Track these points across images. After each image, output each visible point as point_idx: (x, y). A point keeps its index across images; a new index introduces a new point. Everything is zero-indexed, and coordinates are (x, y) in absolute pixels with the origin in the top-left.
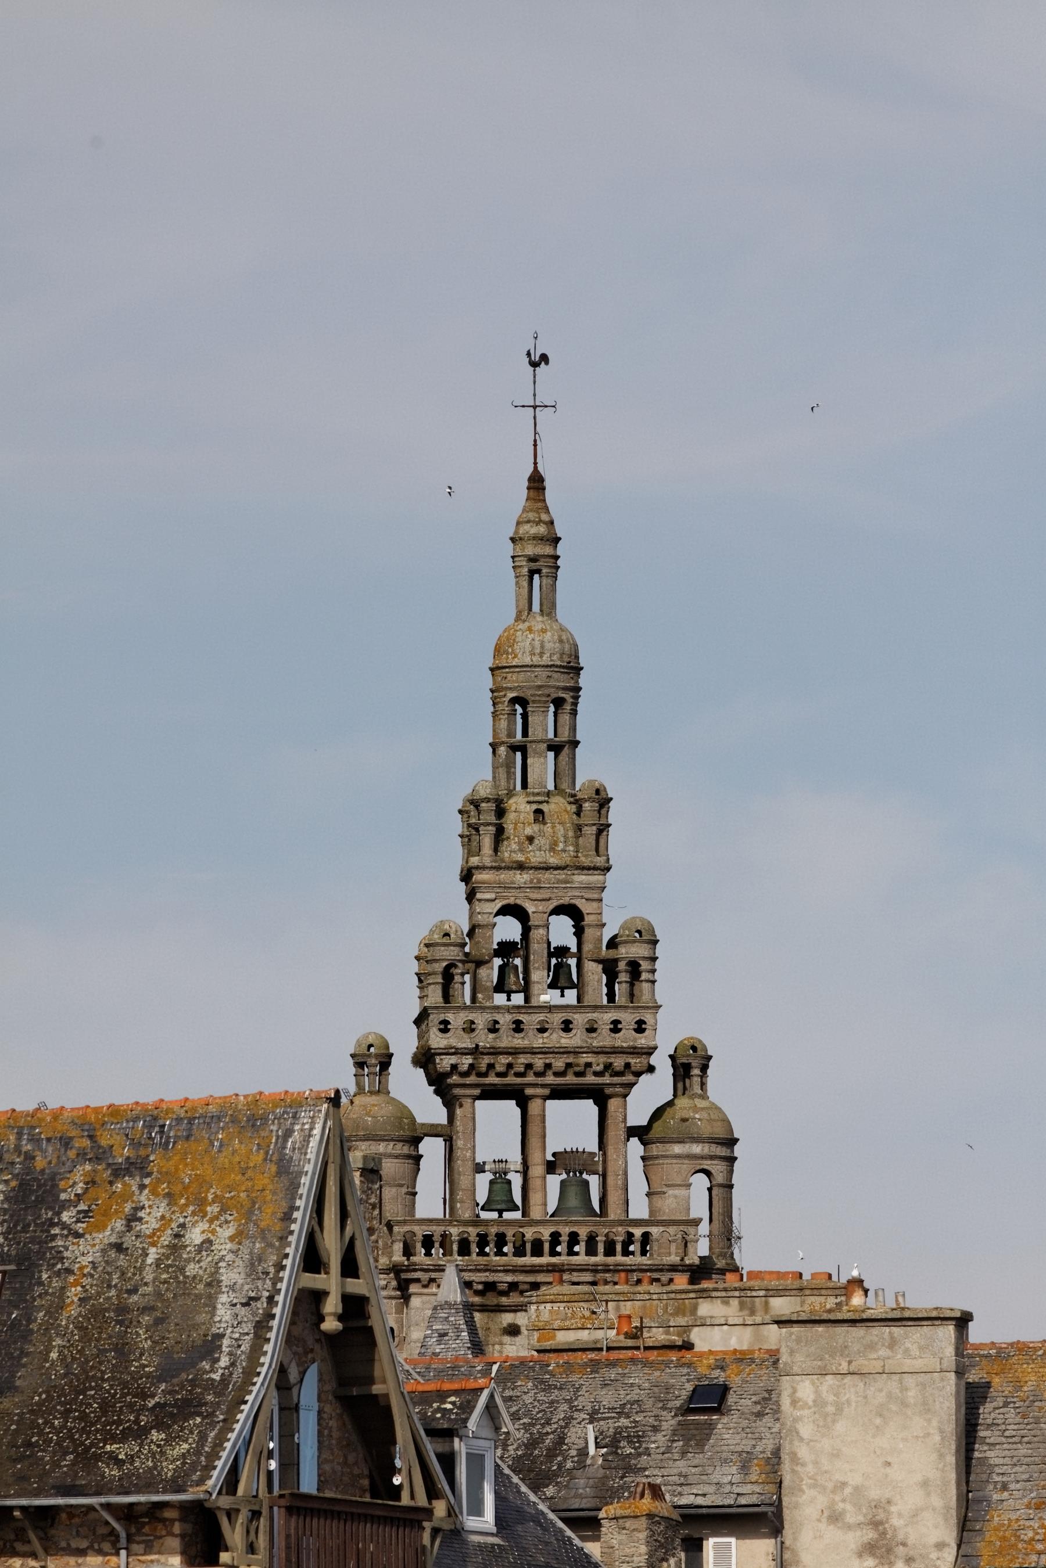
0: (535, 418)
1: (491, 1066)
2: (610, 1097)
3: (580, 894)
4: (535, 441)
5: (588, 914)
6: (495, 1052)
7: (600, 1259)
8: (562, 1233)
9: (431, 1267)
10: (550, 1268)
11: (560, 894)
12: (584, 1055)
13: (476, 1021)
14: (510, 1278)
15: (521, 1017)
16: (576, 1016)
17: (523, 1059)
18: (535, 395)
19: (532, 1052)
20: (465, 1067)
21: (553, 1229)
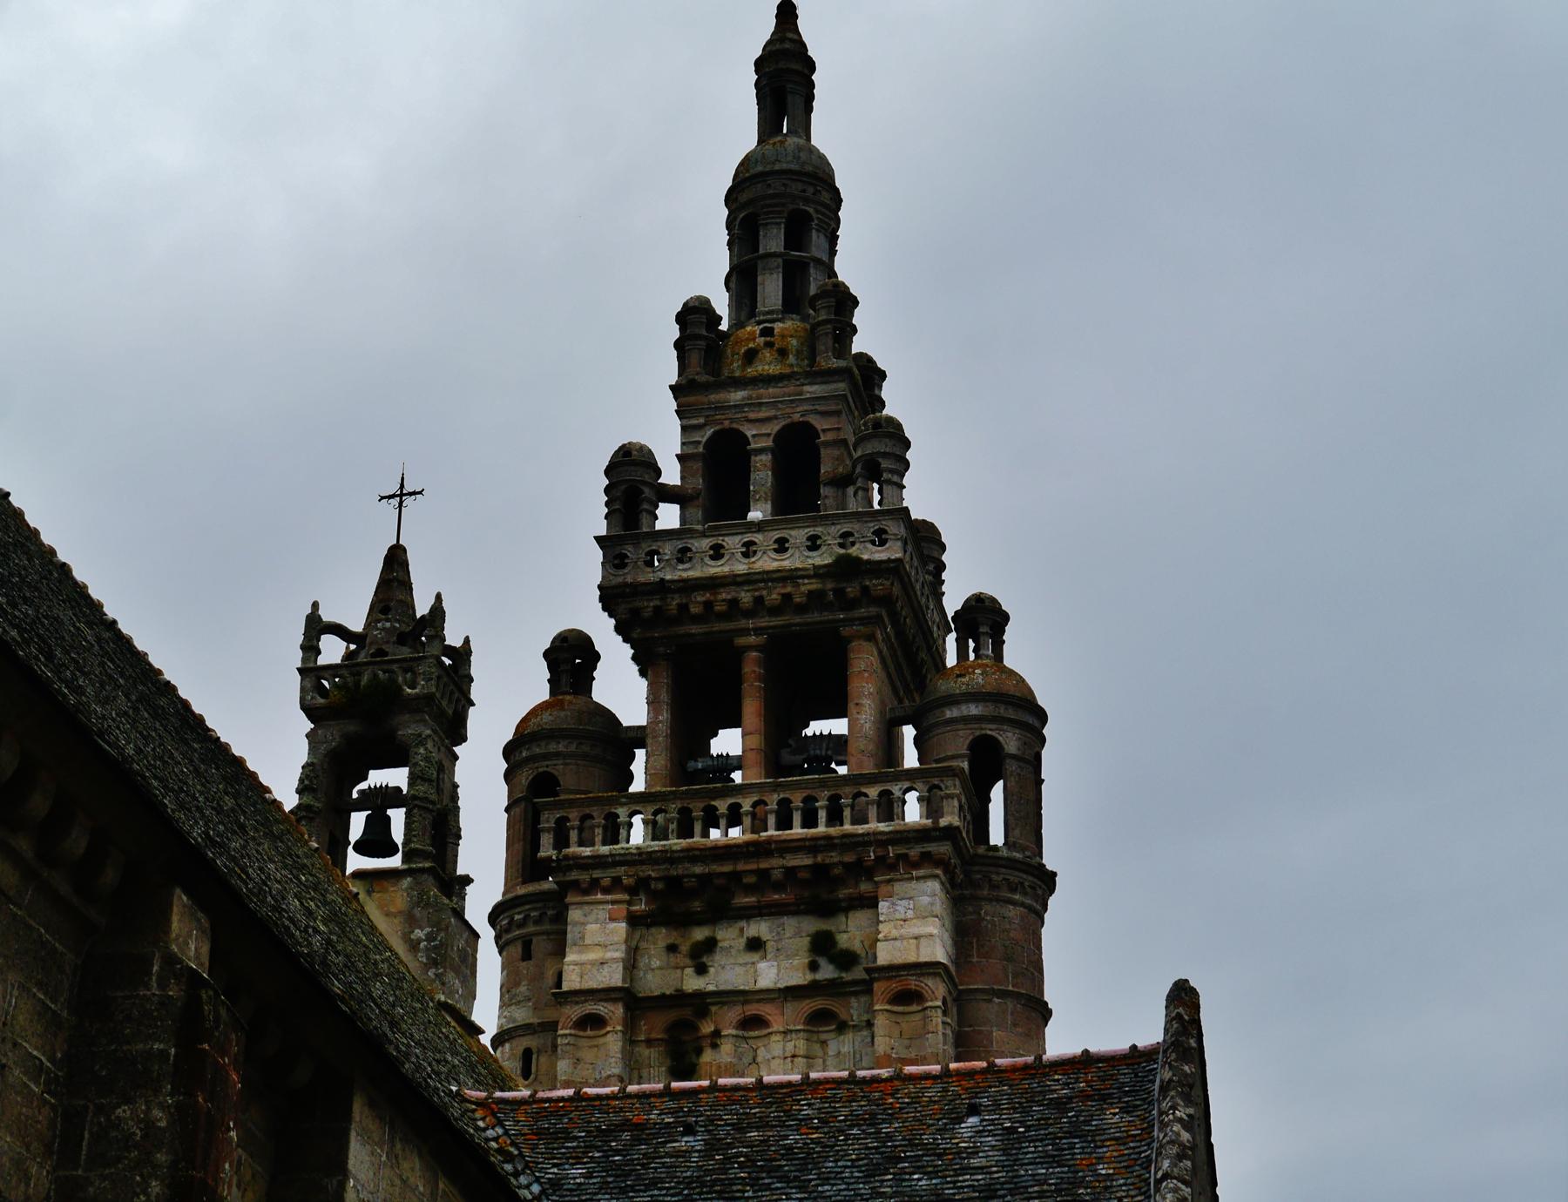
1: (683, 608)
2: (849, 640)
3: (812, 408)
7: (821, 829)
10: (751, 849)
11: (788, 410)
12: (806, 581)
13: (661, 550)
14: (698, 869)
16: (793, 533)
17: (724, 595)
19: (734, 581)
20: (647, 614)
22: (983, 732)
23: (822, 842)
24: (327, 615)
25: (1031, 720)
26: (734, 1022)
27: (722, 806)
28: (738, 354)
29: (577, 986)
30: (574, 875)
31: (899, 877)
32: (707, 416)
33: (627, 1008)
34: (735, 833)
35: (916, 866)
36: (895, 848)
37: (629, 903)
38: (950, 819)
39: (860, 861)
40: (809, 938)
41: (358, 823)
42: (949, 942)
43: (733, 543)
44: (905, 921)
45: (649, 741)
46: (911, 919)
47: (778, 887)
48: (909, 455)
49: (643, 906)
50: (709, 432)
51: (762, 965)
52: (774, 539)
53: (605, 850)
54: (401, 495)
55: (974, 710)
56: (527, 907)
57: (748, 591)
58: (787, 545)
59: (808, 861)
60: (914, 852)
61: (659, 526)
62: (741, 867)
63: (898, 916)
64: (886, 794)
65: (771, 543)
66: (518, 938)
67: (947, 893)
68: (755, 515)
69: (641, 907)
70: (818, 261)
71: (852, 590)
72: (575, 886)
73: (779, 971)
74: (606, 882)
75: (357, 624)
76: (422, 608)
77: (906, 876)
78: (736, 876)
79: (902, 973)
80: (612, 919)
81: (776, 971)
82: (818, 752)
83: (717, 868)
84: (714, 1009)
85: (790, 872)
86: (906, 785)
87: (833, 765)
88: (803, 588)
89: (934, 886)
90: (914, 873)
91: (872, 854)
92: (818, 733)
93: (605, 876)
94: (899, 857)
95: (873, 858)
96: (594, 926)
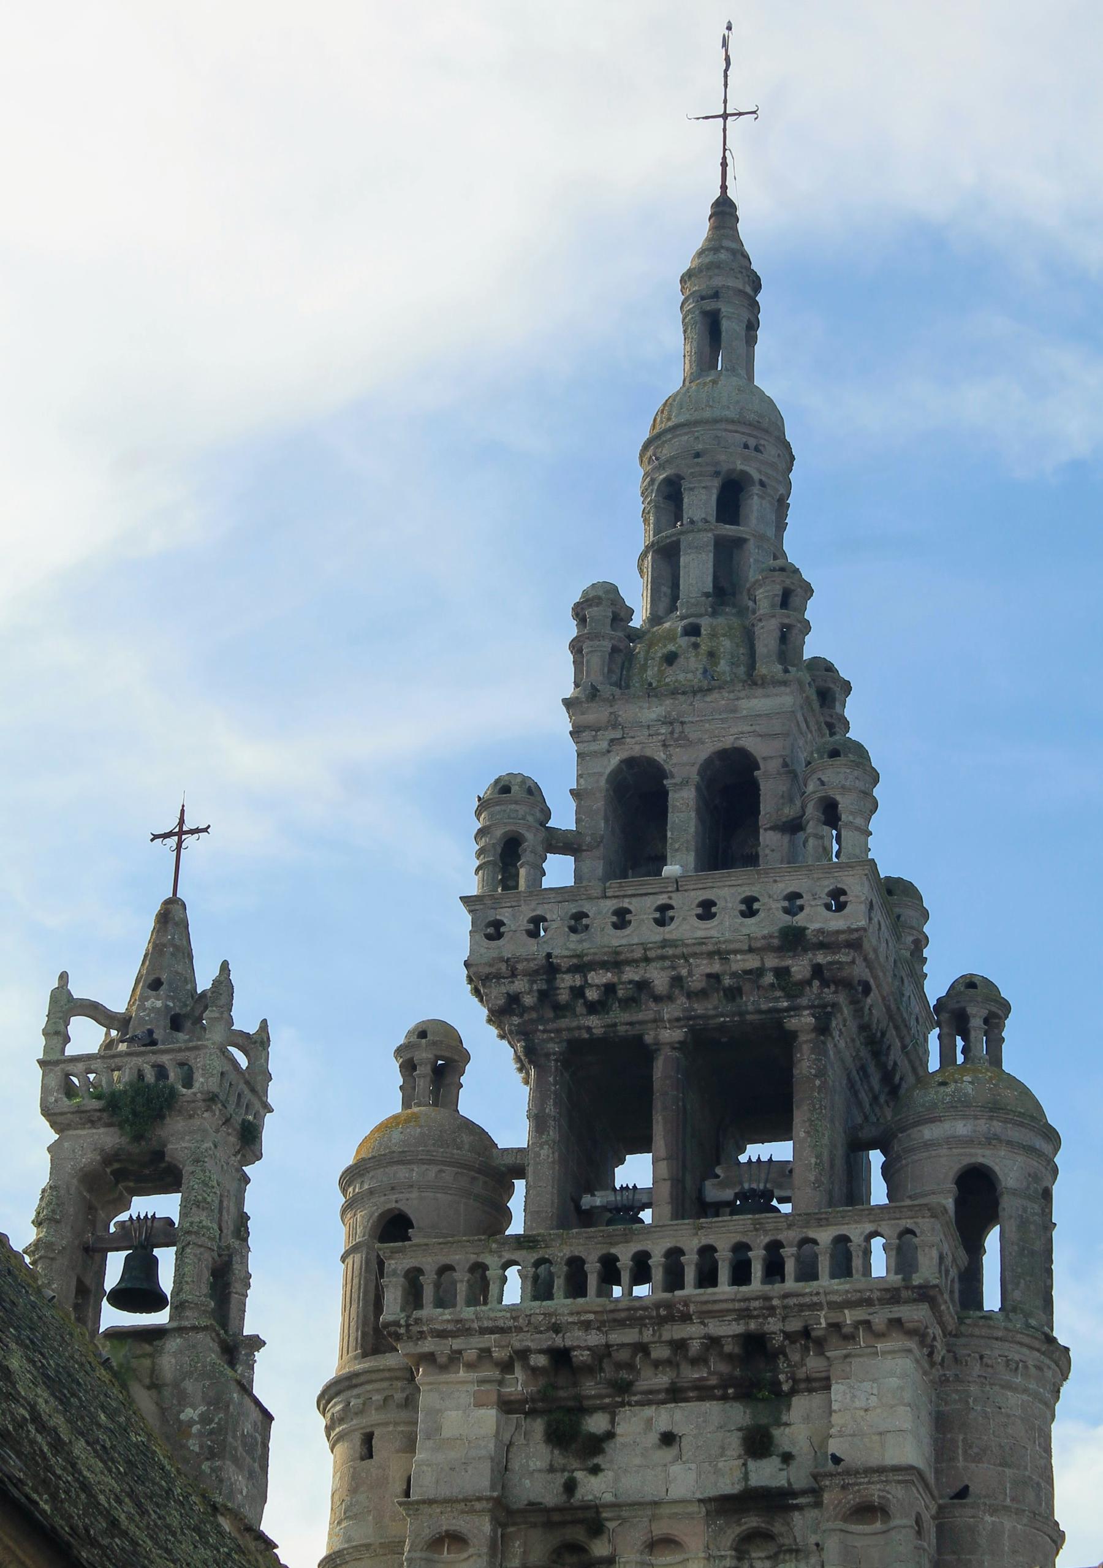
0: (725, 130)
1: (578, 992)
4: (724, 158)
5: (764, 759)
6: (581, 967)
8: (685, 1249)
9: (450, 1327)
10: (663, 1312)
12: (739, 957)
13: (548, 917)
14: (594, 1339)
15: (626, 903)
16: (725, 892)
18: (725, 101)
21: (668, 1244)
22: (973, 1160)
23: (756, 1304)
24: (79, 990)
25: (1040, 1143)
26: (639, 1543)
27: (625, 1255)
28: (653, 659)
29: (431, 1494)
30: (428, 1345)
31: (858, 1352)
32: (612, 740)
33: (497, 1523)
34: (642, 1291)
35: (880, 1336)
36: (853, 1312)
37: (501, 1383)
38: (927, 1271)
39: (806, 1333)
40: (740, 1434)
41: (115, 1265)
42: (927, 1440)
43: (643, 908)
44: (866, 1410)
45: (530, 1170)
46: (875, 1408)
47: (698, 1361)
48: (877, 792)
49: (520, 1388)
50: (614, 760)
51: (676, 1469)
52: (697, 902)
53: (468, 1313)
54: (181, 833)
55: (961, 1128)
56: (369, 1387)
57: (663, 969)
58: (714, 910)
59: (738, 1328)
60: (880, 1317)
61: (547, 883)
62: (648, 1335)
63: (857, 1404)
64: (842, 1241)
65: (694, 906)
66: (354, 1430)
67: (925, 1373)
68: (671, 870)
69: (518, 1384)
70: (761, 537)
71: (800, 967)
72: (429, 1358)
73: (699, 1475)
74: (471, 1355)
75: (118, 1004)
76: (204, 981)
77: (869, 1350)
78: (642, 1348)
79: (862, 1480)
80: (479, 1405)
81: (695, 1476)
82: (754, 1186)
83: (616, 1337)
84: (611, 1525)
85: (714, 1342)
86: (869, 1228)
87: (774, 1203)
88: (735, 967)
89: (905, 1364)
90: (879, 1346)
91: (823, 1321)
92: (754, 1159)
93: (471, 1346)
94: (857, 1324)
95: (824, 1325)
96: (454, 1413)
